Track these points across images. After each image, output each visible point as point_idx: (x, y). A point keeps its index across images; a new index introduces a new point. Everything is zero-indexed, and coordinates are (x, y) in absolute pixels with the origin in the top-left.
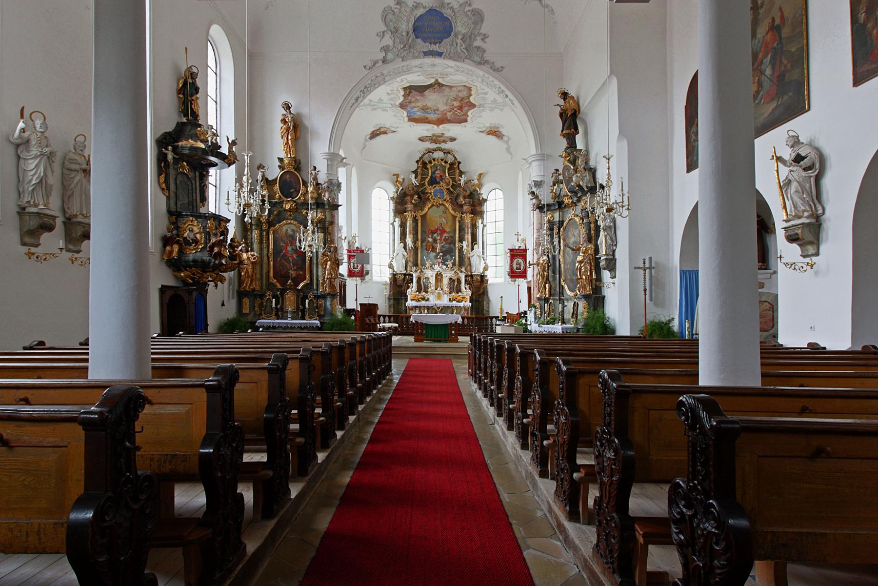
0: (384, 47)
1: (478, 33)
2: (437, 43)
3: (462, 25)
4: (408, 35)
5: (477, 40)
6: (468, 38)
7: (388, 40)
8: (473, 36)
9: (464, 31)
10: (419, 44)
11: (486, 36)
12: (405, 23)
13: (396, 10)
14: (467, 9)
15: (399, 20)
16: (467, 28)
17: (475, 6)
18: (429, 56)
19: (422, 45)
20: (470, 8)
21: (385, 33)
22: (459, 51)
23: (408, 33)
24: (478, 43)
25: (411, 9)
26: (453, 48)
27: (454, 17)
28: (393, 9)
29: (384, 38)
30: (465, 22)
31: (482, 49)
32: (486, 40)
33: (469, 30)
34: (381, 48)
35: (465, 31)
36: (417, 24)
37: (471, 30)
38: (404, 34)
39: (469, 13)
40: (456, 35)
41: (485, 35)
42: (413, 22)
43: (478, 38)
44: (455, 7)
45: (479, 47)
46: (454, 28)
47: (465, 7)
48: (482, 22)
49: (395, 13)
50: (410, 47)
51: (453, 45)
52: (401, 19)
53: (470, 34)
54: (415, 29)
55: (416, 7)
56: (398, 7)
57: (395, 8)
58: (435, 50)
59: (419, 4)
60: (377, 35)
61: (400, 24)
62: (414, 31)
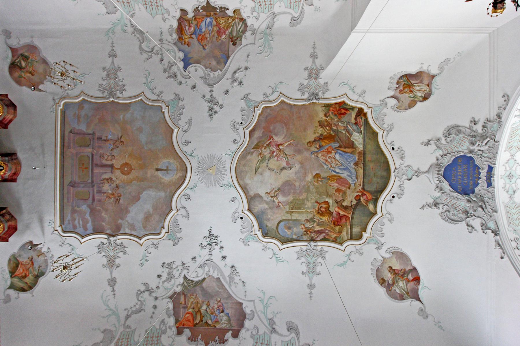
0: (482, 229)
1: (469, 129)
2: (479, 171)
3: (460, 146)
4: (470, 202)
5: (476, 129)
6: (474, 137)
7: (476, 223)
8: (472, 134)
9: (467, 144)
10: (480, 191)
11: (472, 120)
12: (458, 202)
13: (445, 209)
14: (443, 141)
15: (456, 208)
16: (464, 140)
17: (440, 134)
18: (492, 181)
19: (481, 188)
20: (443, 139)
21: (469, 223)
22: (487, 147)
23: (469, 201)
24: (479, 128)
25: (443, 194)
26: (484, 154)
27: (452, 154)
28: (443, 211)
29: (474, 226)
30: (458, 143)
31: (485, 123)
32: (476, 120)
33: (466, 138)
34: (484, 232)
35: (467, 142)
36: (460, 190)
37: (466, 137)
38: (469, 205)
39: (449, 140)
40: (471, 152)
41: (471, 122)
42: (457, 193)
43: (474, 129)
44: (441, 153)
45: (483, 126)
46: (463, 154)
47: (442, 144)
48: (458, 126)
49: (448, 210)
50: (483, 201)
51: (481, 154)
52: (454, 205)
53: (469, 138)
54: (465, 193)
55: (441, 189)
56: (441, 206)
57: (443, 209)
58: (486, 174)
59: (437, 187)
60: (471, 233)
61: (460, 207)
62: (465, 194)
